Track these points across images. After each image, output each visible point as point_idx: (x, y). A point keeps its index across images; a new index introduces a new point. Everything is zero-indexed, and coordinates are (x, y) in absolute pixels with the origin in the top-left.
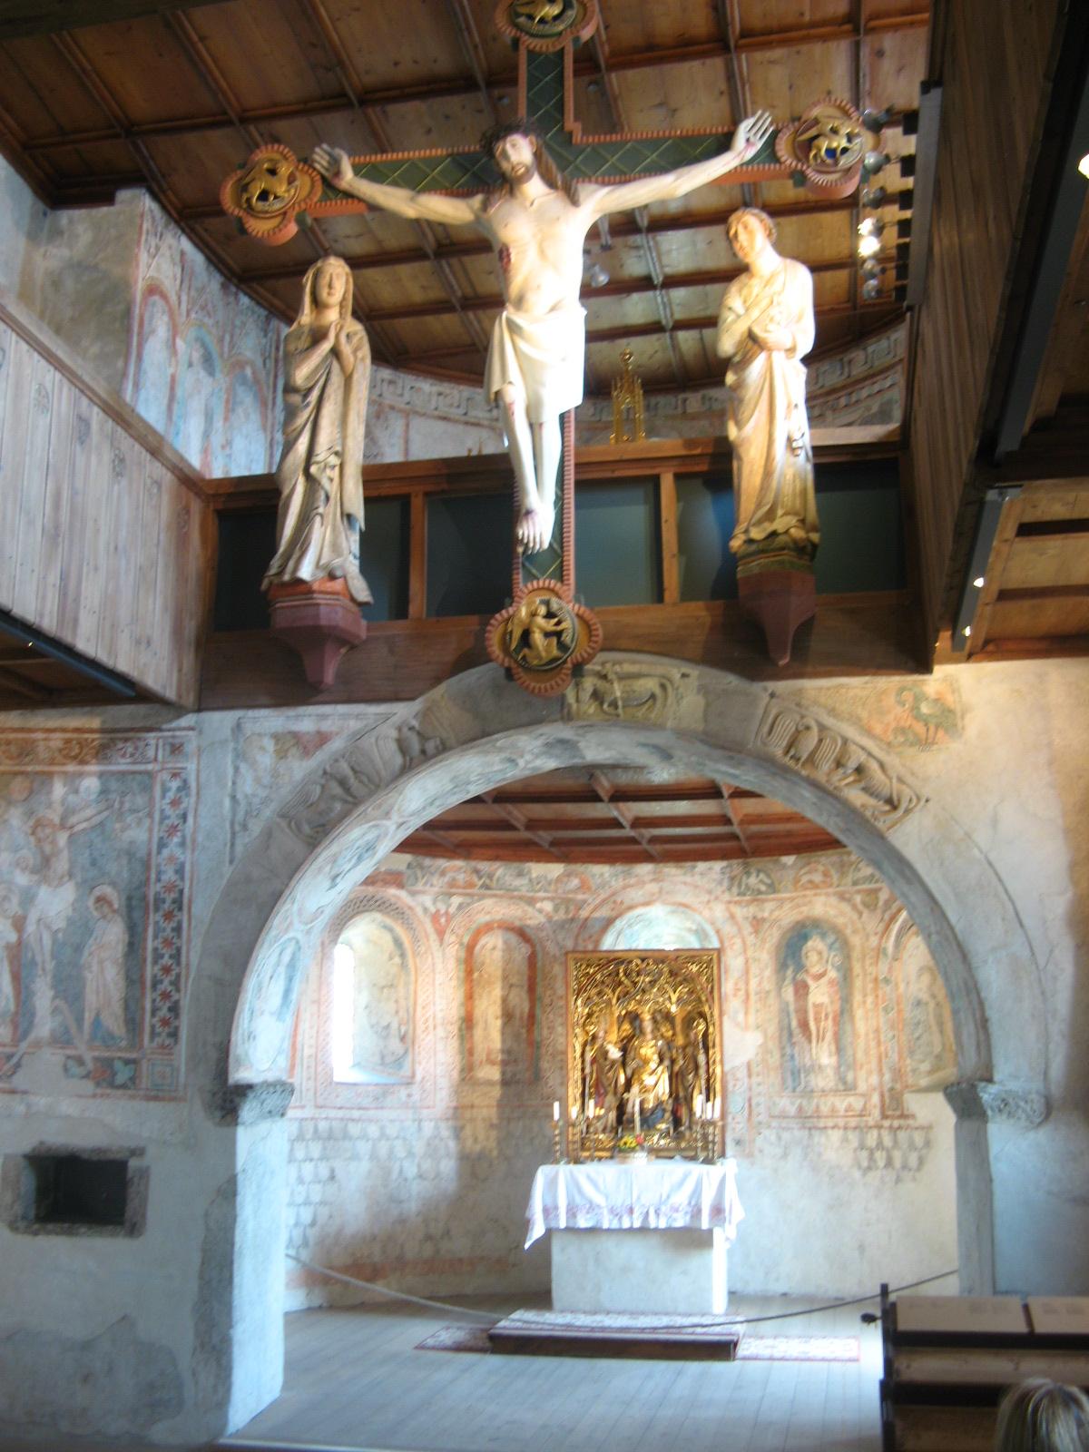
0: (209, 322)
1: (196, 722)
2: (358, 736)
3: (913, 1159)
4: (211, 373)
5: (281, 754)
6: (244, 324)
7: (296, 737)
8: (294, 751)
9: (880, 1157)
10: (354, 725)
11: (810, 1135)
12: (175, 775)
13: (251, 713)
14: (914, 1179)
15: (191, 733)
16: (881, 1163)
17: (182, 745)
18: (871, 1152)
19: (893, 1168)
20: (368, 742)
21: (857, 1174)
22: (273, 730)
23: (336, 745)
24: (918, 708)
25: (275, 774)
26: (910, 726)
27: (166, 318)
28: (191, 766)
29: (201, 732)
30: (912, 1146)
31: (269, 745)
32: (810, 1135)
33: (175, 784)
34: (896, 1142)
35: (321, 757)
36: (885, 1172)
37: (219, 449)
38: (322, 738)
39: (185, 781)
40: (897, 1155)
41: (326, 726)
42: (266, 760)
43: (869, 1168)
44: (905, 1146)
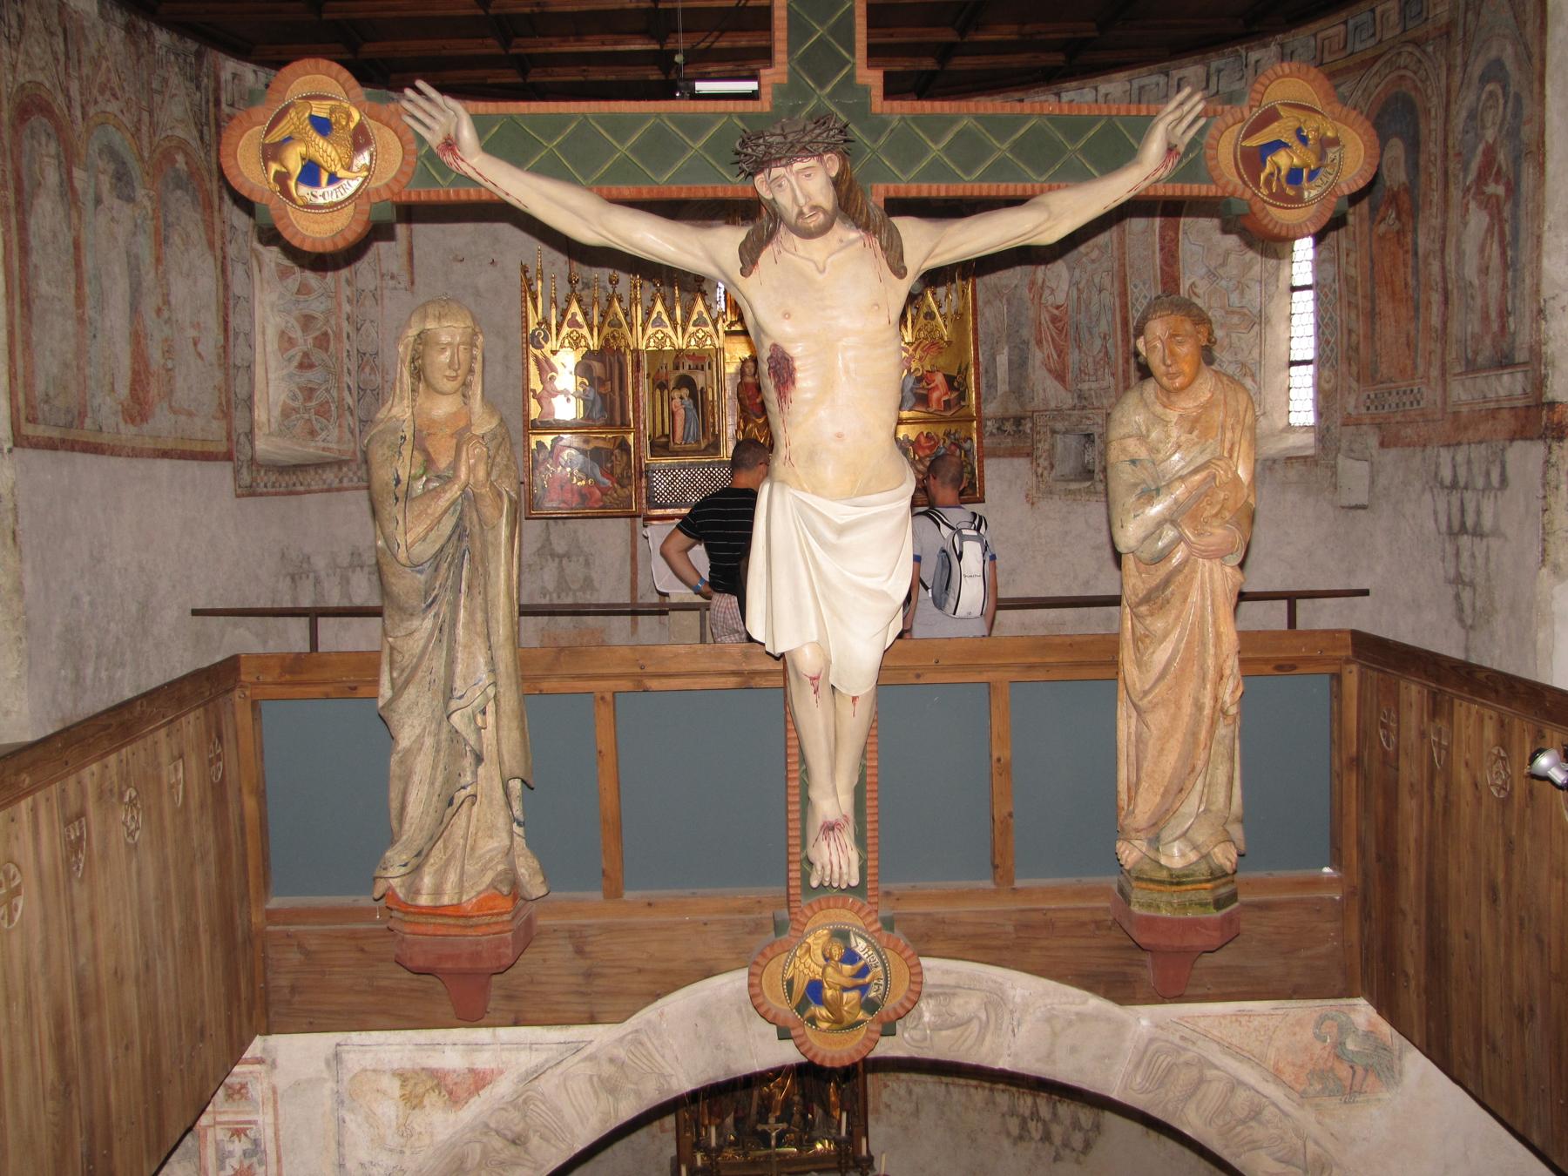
0: (113, 107)
1: (264, 1049)
2: (535, 1074)
3: (1077, 1139)
4: (130, 199)
5: (413, 1101)
6: (165, 81)
7: (437, 1079)
8: (432, 1098)
9: (1035, 1129)
10: (528, 1060)
11: (948, 1092)
12: (238, 1133)
13: (355, 1037)
14: (1078, 1162)
15: (257, 1067)
16: (1037, 1136)
17: (243, 1086)
18: (1024, 1122)
19: (1051, 1143)
20: (547, 1084)
21: (1006, 1143)
22: (396, 1066)
23: (503, 1088)
24: (1343, 1044)
25: (405, 1131)
26: (1332, 1069)
27: (53, 148)
28: (264, 1119)
29: (274, 1065)
30: (1076, 1125)
31: (393, 1087)
32: (948, 1092)
33: (238, 1147)
34: (1055, 1114)
35: (474, 1109)
36: (1040, 1145)
37: (154, 315)
38: (479, 1080)
39: (256, 1142)
40: (1056, 1130)
41: (483, 1061)
42: (389, 1110)
43: (1021, 1138)
44: (1067, 1122)
